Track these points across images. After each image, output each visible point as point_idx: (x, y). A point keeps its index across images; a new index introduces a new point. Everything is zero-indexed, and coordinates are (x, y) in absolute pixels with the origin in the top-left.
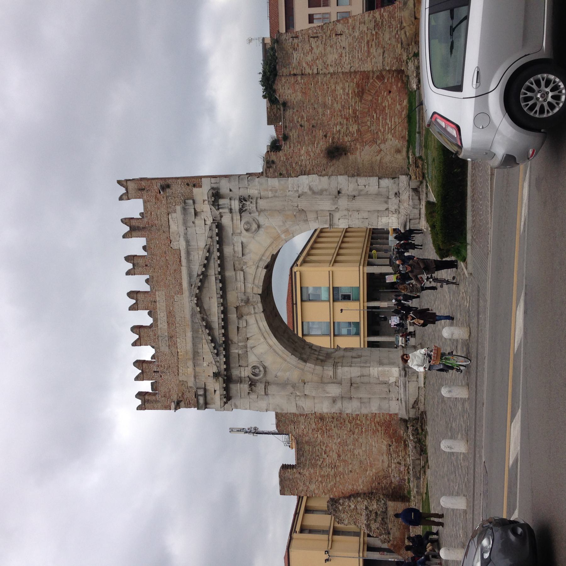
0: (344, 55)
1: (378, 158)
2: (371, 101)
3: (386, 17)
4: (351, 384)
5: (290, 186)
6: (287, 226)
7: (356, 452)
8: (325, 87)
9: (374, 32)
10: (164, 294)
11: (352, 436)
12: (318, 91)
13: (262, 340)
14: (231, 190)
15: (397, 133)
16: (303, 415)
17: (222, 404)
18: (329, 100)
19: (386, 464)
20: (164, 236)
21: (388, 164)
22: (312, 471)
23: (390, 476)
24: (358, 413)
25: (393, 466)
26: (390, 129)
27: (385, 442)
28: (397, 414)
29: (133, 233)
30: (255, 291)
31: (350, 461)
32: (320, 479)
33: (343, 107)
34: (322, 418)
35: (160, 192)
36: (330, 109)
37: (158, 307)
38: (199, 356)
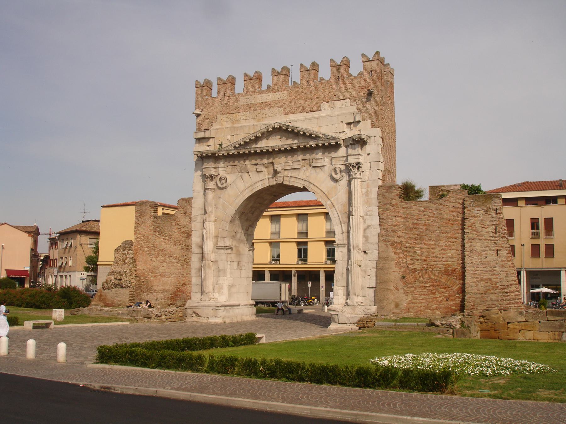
0: (480, 257)
1: (392, 288)
2: (440, 282)
3: (510, 296)
5: (371, 208)
6: (336, 207)
7: (164, 264)
8: (454, 240)
9: (498, 285)
10: (285, 98)
11: (175, 261)
12: (451, 233)
13: (248, 185)
14: (368, 154)
15: (411, 305)
16: (190, 221)
17: (196, 153)
18: (442, 243)
19: (156, 289)
22: (151, 228)
24: (192, 266)
25: (155, 294)
26: (416, 298)
27: (171, 288)
28: (191, 298)
29: (334, 69)
30: (286, 179)
31: (158, 259)
32: (146, 235)
33: (436, 257)
34: (189, 236)
36: (435, 244)
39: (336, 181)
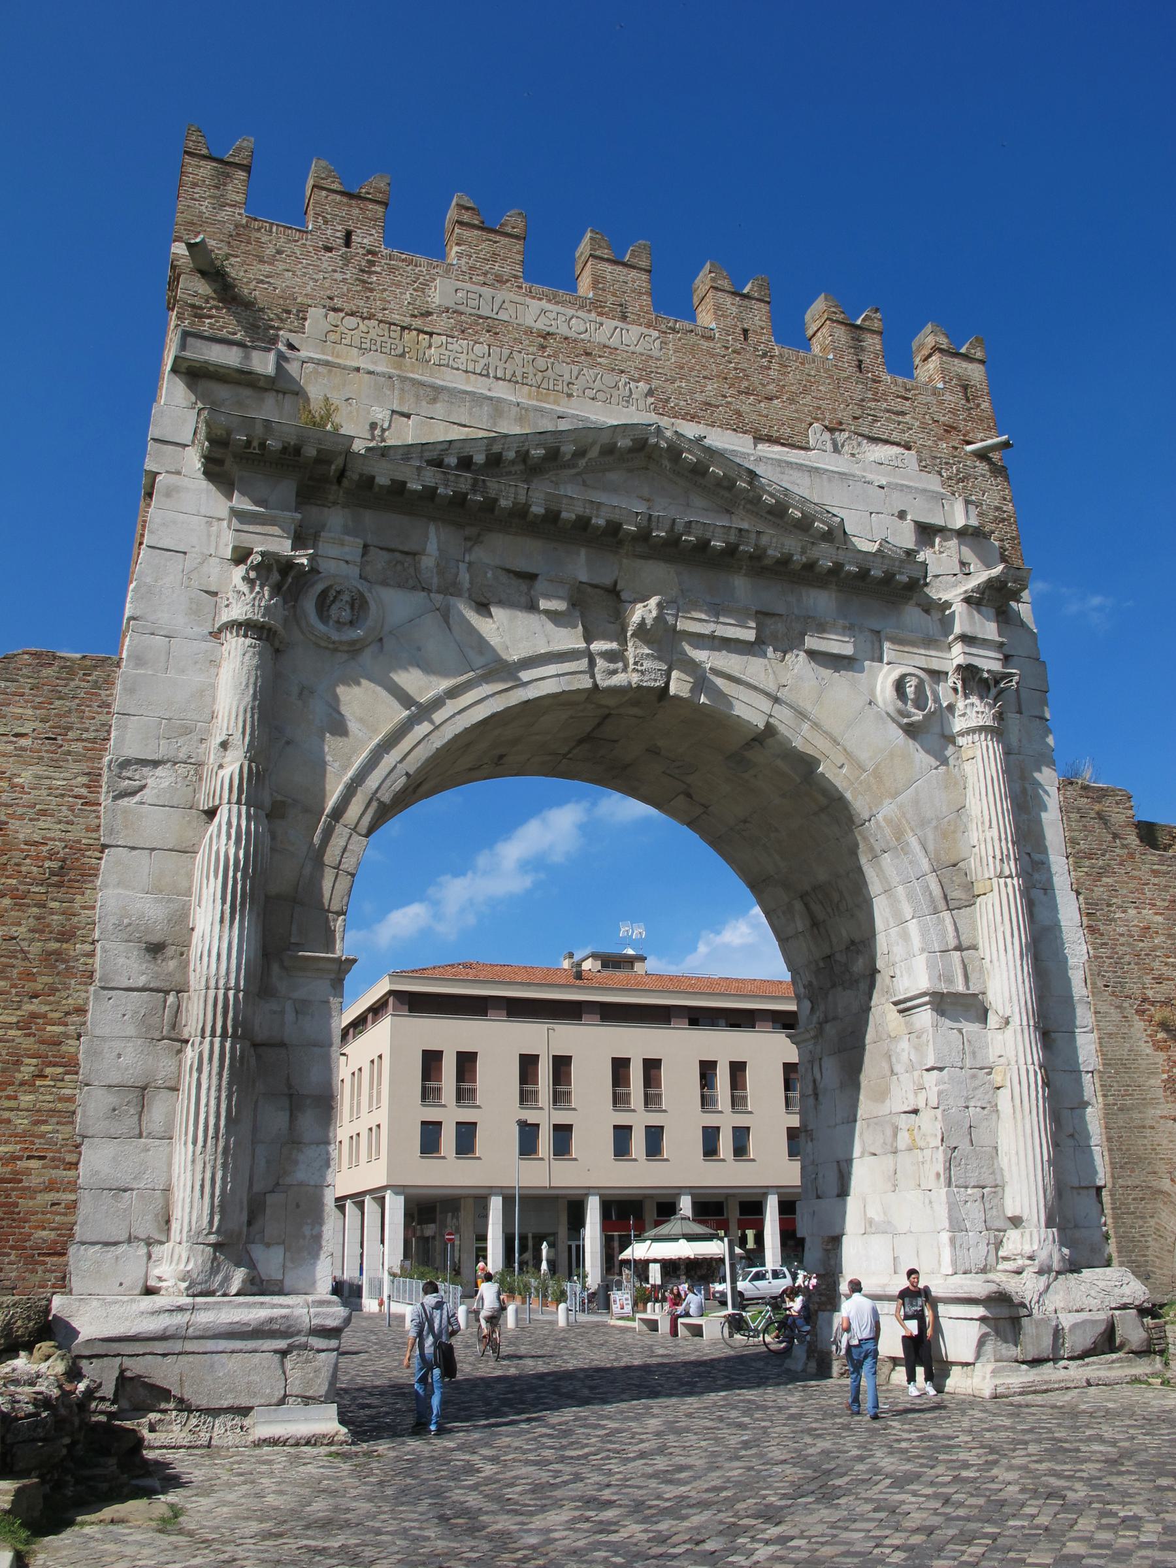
1: (1166, 1185)
4: (255, 1045)
20: (844, 415)
21: (1152, 1222)
34: (71, 871)
35: (969, 443)
37: (603, 319)
38: (417, 396)
39: (911, 730)
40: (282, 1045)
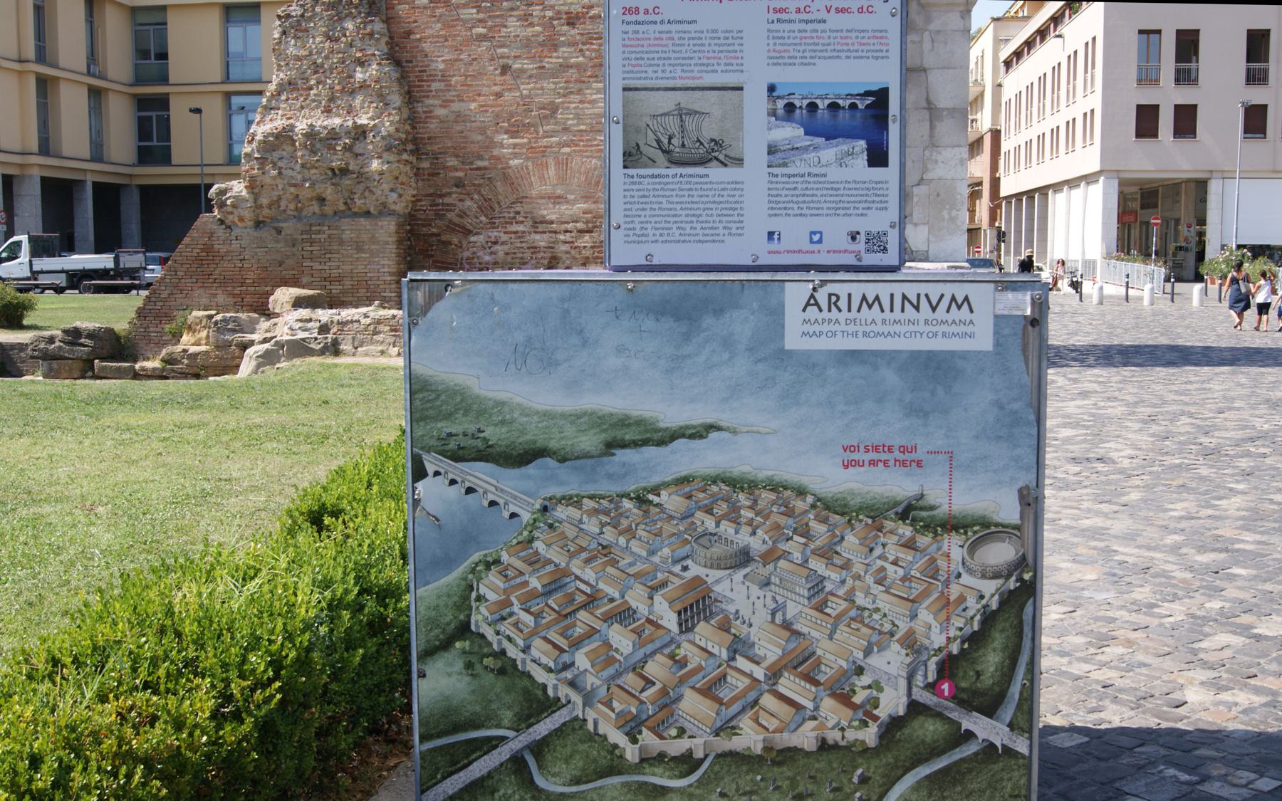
23: (493, 226)
31: (552, 61)
40: (925, 70)
